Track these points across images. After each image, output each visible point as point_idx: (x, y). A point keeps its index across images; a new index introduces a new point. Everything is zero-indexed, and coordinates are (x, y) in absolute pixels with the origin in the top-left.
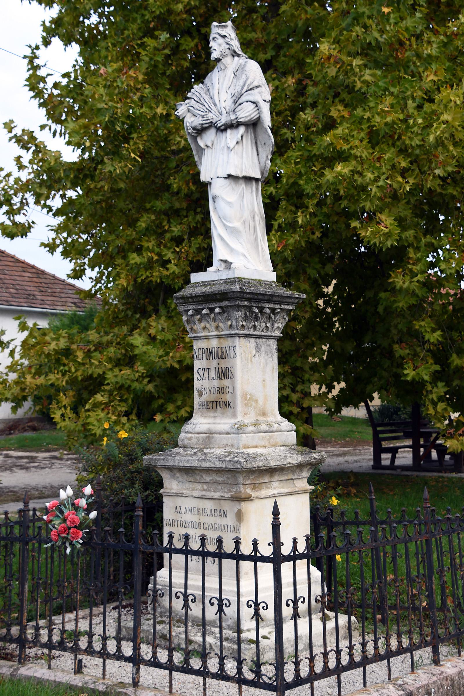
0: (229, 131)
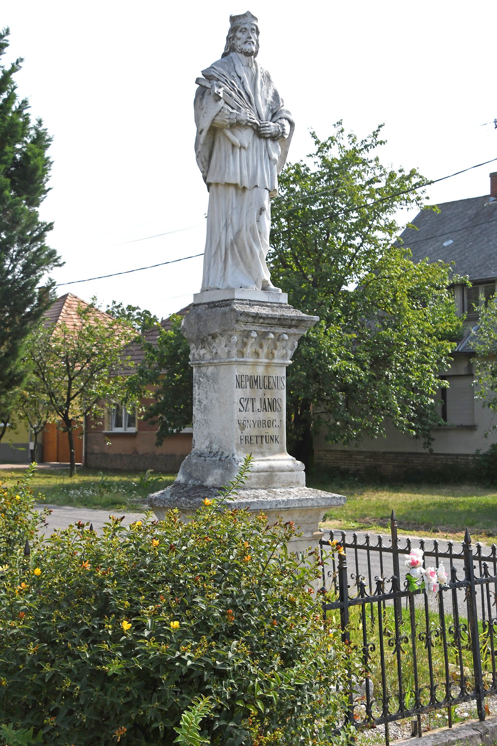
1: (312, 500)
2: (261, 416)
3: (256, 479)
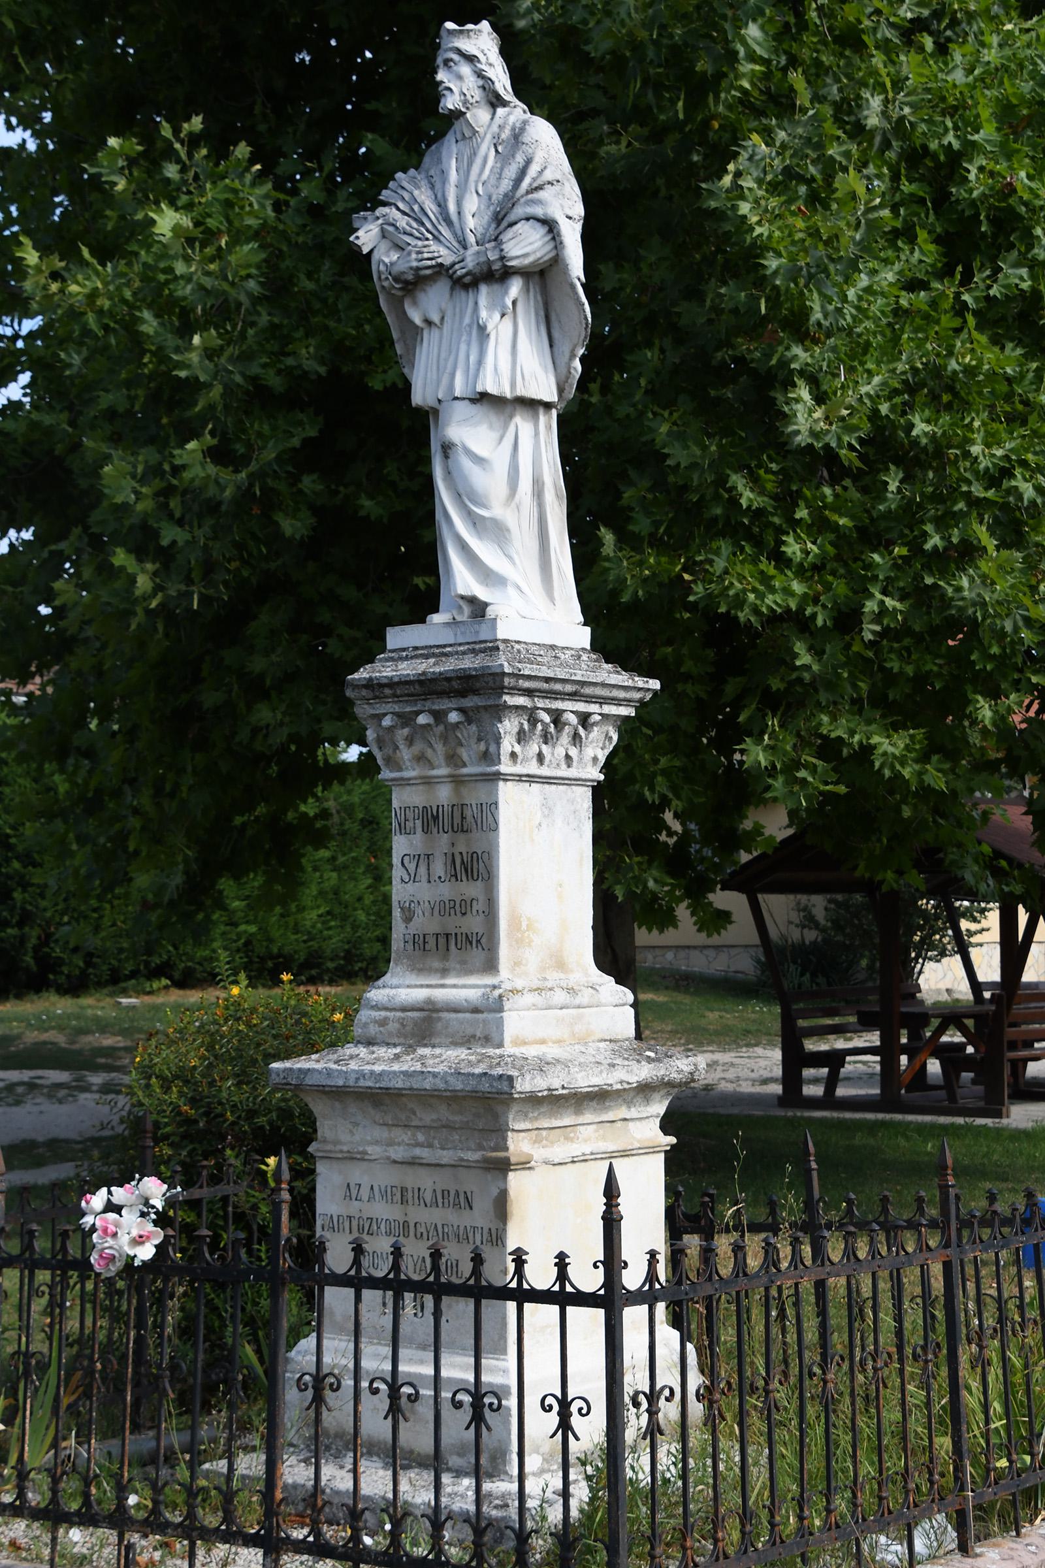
0: (484, 289)
1: (435, 1075)
2: (446, 891)
3: (397, 1025)
